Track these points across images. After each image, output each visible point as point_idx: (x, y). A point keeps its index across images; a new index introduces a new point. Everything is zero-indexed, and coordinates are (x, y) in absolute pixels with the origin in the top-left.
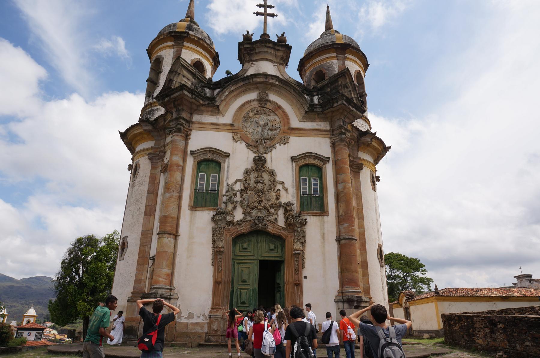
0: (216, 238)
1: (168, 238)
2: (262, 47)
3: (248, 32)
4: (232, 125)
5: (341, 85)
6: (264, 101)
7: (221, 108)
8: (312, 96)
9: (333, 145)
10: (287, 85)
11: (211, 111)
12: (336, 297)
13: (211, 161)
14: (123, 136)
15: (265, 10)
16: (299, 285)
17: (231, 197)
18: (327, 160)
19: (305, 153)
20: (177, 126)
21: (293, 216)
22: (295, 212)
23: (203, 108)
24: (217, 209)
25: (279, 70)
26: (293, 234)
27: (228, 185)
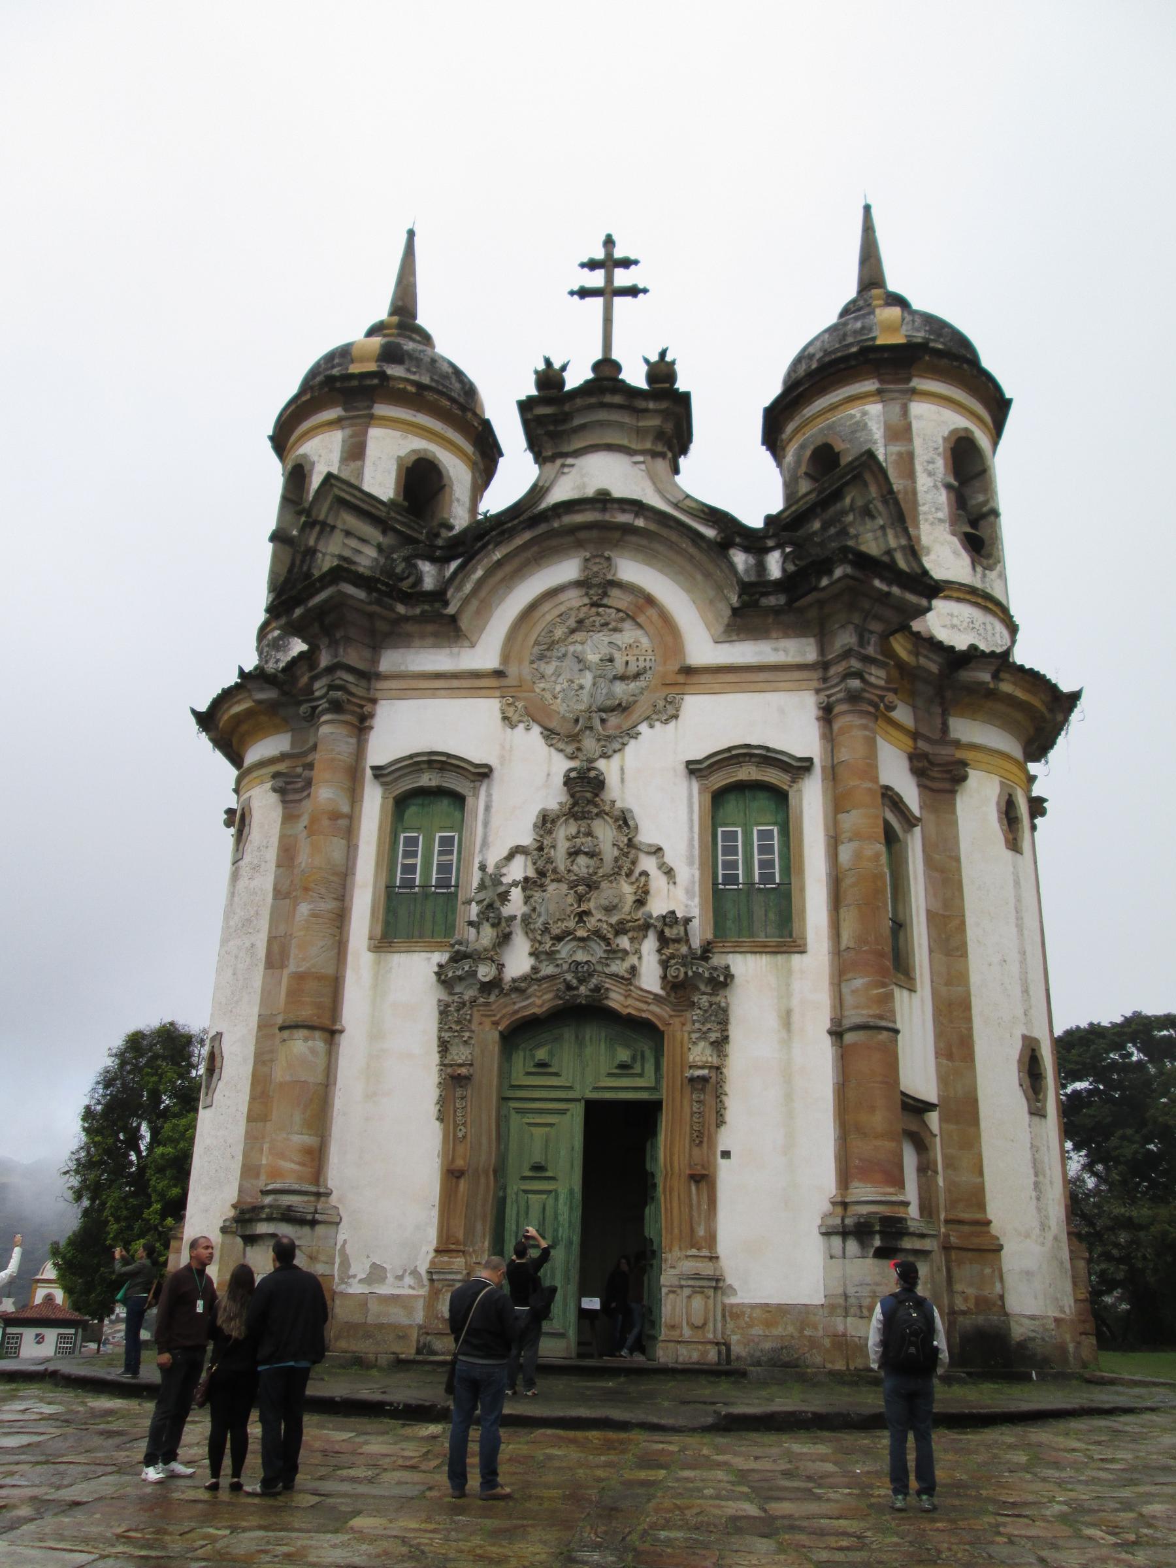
0: (446, 1035)
1: (306, 1039)
2: (590, 408)
3: (548, 363)
4: (498, 674)
5: (852, 508)
6: (599, 585)
7: (464, 623)
9: (827, 714)
10: (670, 527)
11: (435, 635)
12: (825, 1217)
13: (437, 789)
14: (206, 720)
15: (609, 279)
16: (704, 1179)
17: (490, 906)
19: (729, 749)
20: (327, 693)
21: (684, 957)
22: (696, 943)
23: (409, 627)
24: (452, 946)
25: (653, 477)
26: (688, 1015)
27: (483, 868)
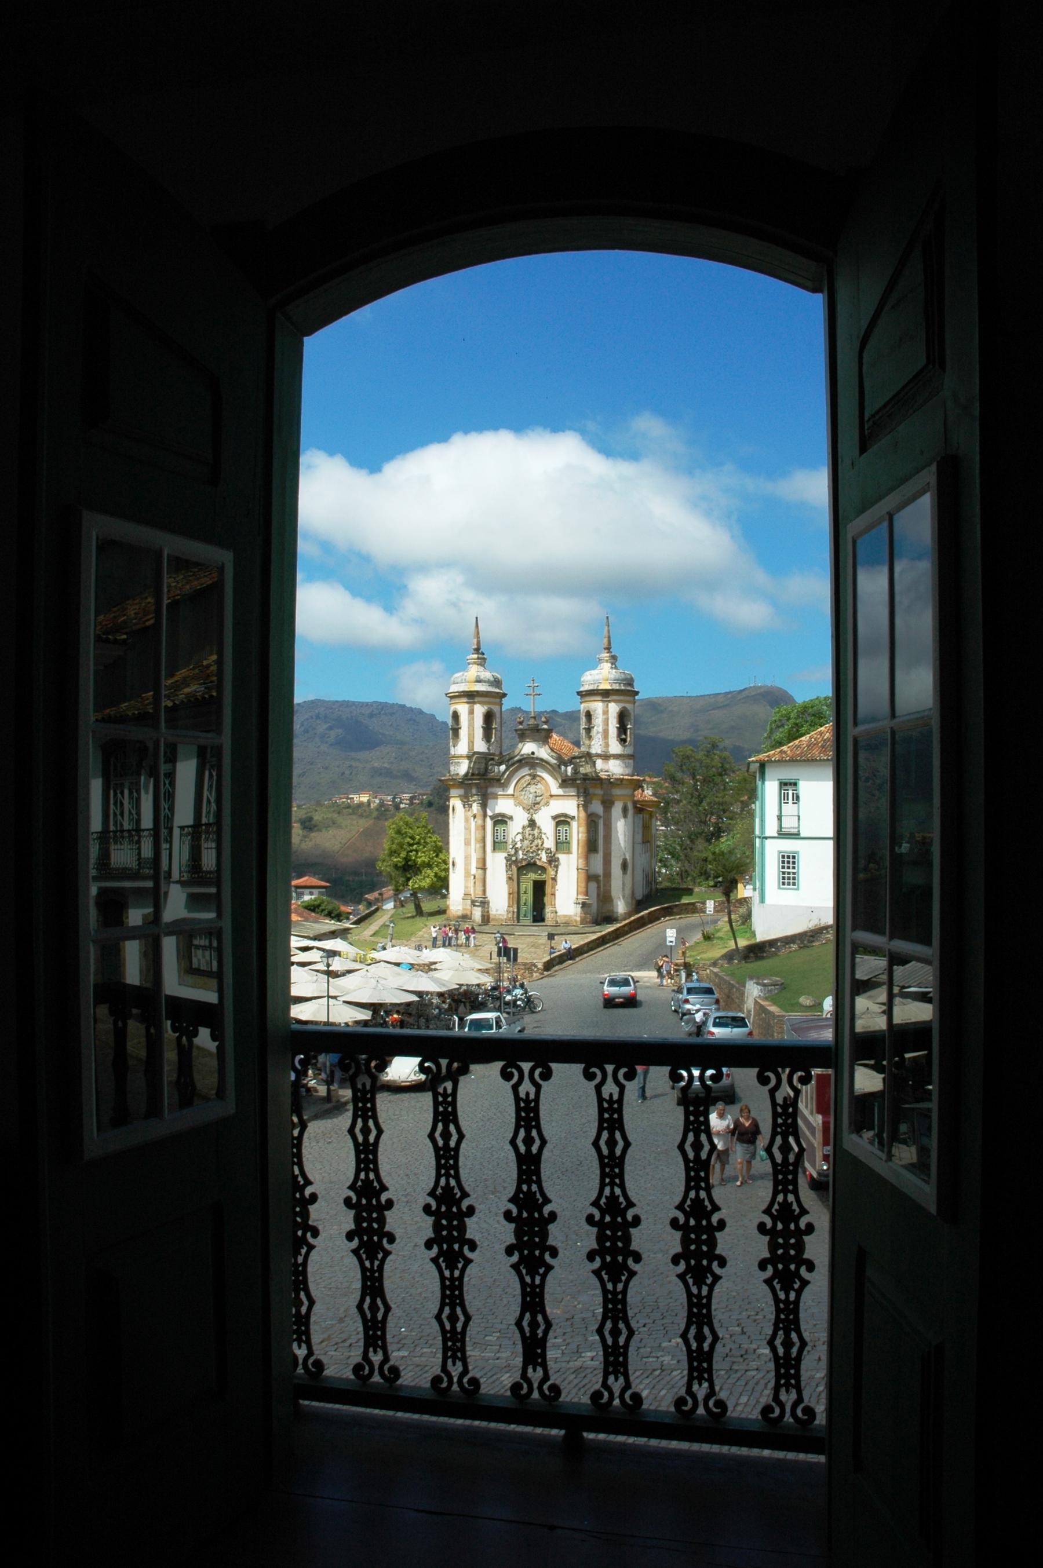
8: (566, 766)
16: (554, 894)
18: (573, 818)
